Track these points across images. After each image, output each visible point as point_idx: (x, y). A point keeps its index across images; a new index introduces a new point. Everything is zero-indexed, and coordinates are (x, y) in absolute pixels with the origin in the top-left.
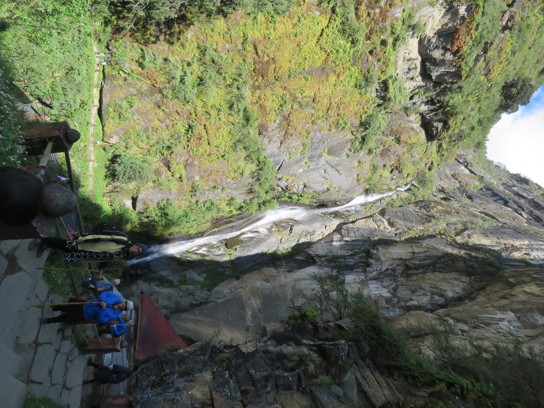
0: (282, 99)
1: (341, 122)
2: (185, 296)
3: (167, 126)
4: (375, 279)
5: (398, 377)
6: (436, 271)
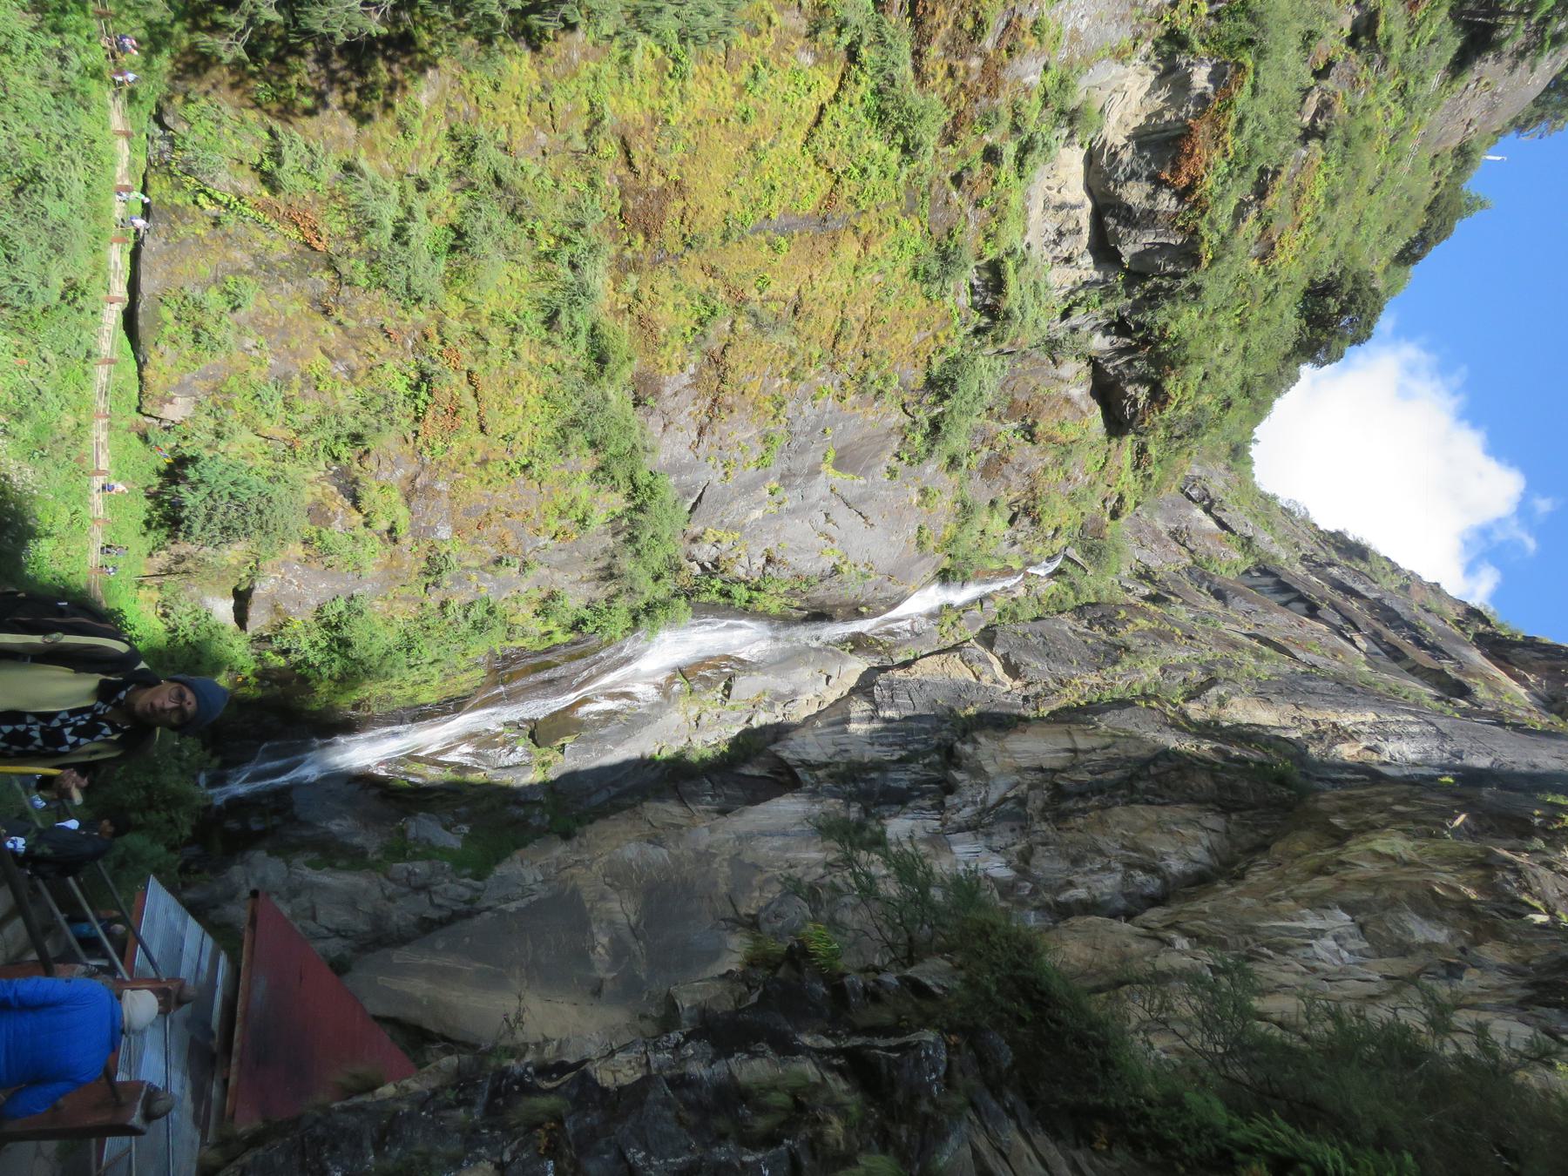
0: (705, 303)
1: (873, 375)
2: (404, 895)
3: (352, 373)
4: (969, 829)
5: (1110, 1146)
6: (1136, 802)
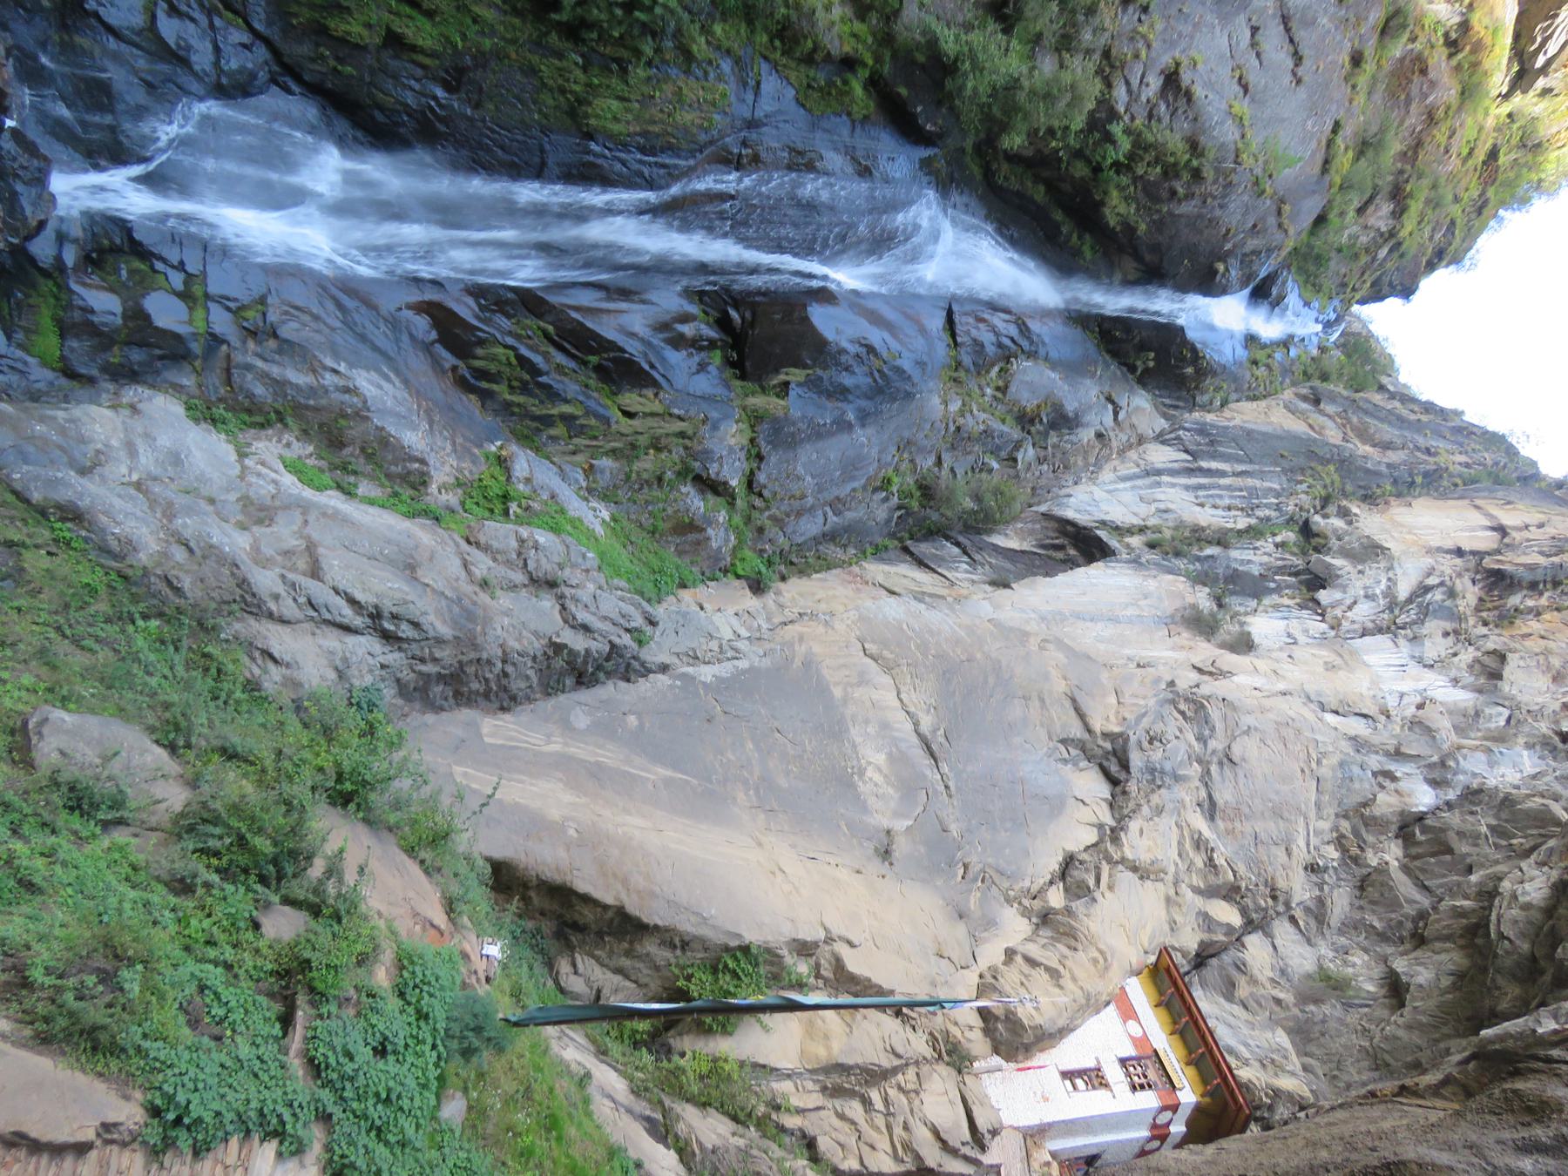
2: (513, 587)
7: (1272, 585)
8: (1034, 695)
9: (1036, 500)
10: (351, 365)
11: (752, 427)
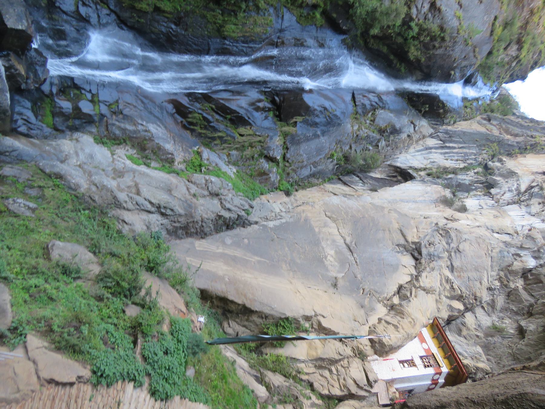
2: (204, 196)
4: (514, 203)
7: (473, 188)
8: (387, 229)
9: (386, 160)
10: (147, 122)
11: (284, 138)
